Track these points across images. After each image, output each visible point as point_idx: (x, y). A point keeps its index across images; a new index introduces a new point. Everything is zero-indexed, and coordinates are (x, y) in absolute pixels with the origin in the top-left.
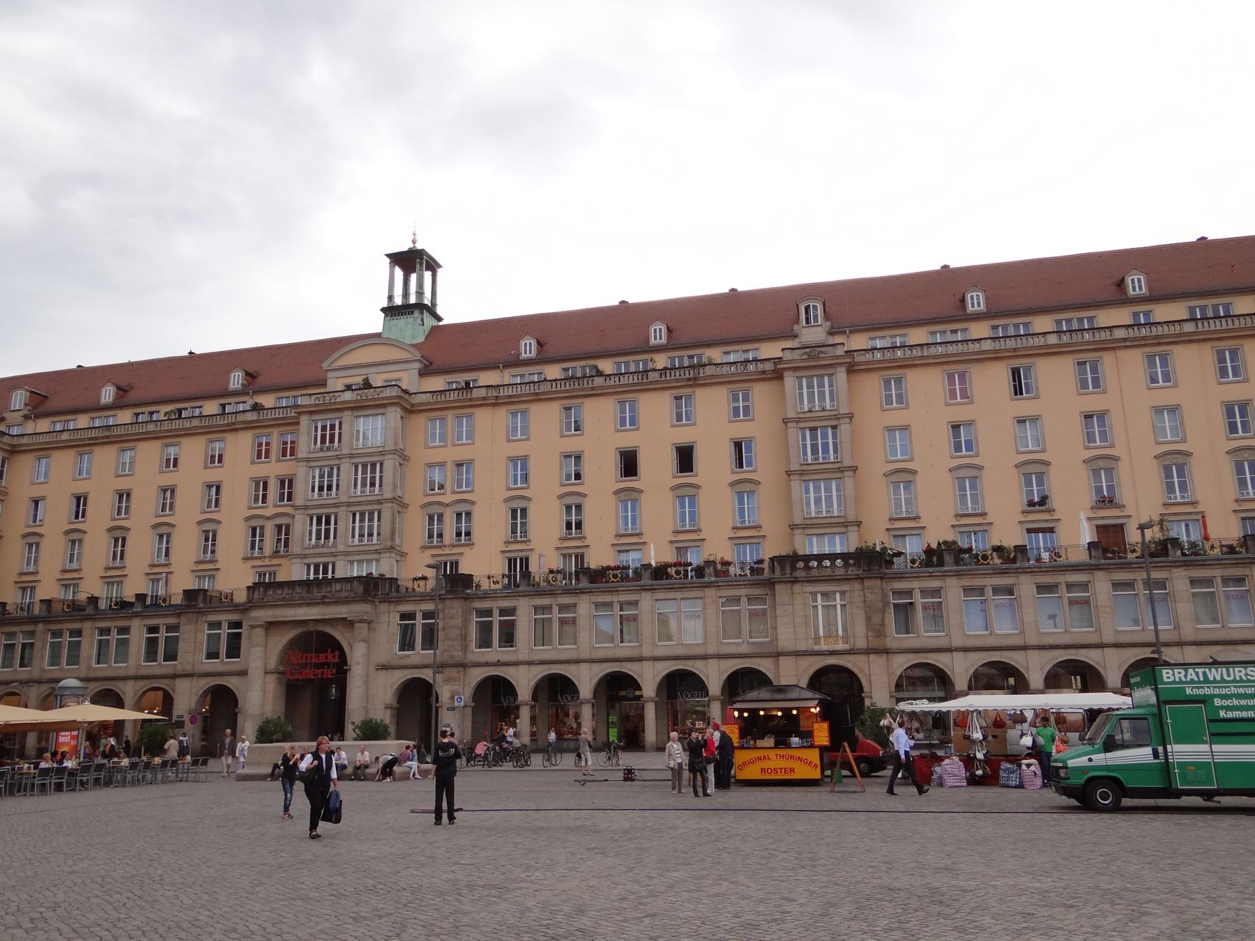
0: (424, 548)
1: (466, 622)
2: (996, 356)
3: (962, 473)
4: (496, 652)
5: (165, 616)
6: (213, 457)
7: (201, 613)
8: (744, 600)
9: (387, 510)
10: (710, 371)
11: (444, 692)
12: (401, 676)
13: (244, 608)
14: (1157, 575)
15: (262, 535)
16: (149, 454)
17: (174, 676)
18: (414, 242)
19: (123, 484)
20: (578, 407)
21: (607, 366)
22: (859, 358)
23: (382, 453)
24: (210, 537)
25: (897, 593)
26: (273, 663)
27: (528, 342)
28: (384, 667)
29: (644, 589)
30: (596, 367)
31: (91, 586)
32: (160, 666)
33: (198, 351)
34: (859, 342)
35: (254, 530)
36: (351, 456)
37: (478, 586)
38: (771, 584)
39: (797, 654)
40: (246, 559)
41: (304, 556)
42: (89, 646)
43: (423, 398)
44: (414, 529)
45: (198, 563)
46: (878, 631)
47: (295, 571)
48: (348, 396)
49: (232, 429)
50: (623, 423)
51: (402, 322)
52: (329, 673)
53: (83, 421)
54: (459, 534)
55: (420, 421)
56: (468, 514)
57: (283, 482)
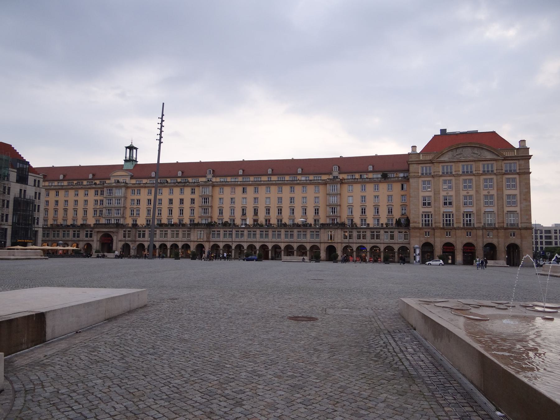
0: (130, 217)
1: (136, 233)
2: (240, 185)
3: (232, 208)
4: (141, 239)
5: (77, 229)
6: (86, 194)
7: (84, 229)
8: (186, 231)
9: (122, 209)
10: (188, 184)
11: (131, 246)
12: (123, 243)
13: (93, 228)
15: (97, 212)
16: (72, 193)
17: (79, 241)
18: (132, 143)
19: (66, 199)
20: (162, 189)
21: (169, 180)
22: (215, 183)
23: (121, 197)
24: (85, 212)
25: (213, 231)
26: (99, 239)
28: (120, 241)
29: (169, 228)
30: (166, 180)
31: (60, 221)
32: (76, 239)
33: (82, 165)
34: (218, 179)
35: (95, 211)
36: (115, 197)
37: (139, 226)
38: (190, 228)
39: (194, 241)
40: (93, 217)
41: (105, 218)
42: (61, 234)
43: (131, 185)
44: (128, 213)
45: (83, 217)
46: (208, 238)
47: (103, 221)
48: (114, 184)
49: (89, 188)
50: (170, 193)
51: (128, 163)
52: (110, 242)
53: (56, 183)
54: (137, 214)
55: (130, 191)
56: (139, 210)
57: (101, 201)
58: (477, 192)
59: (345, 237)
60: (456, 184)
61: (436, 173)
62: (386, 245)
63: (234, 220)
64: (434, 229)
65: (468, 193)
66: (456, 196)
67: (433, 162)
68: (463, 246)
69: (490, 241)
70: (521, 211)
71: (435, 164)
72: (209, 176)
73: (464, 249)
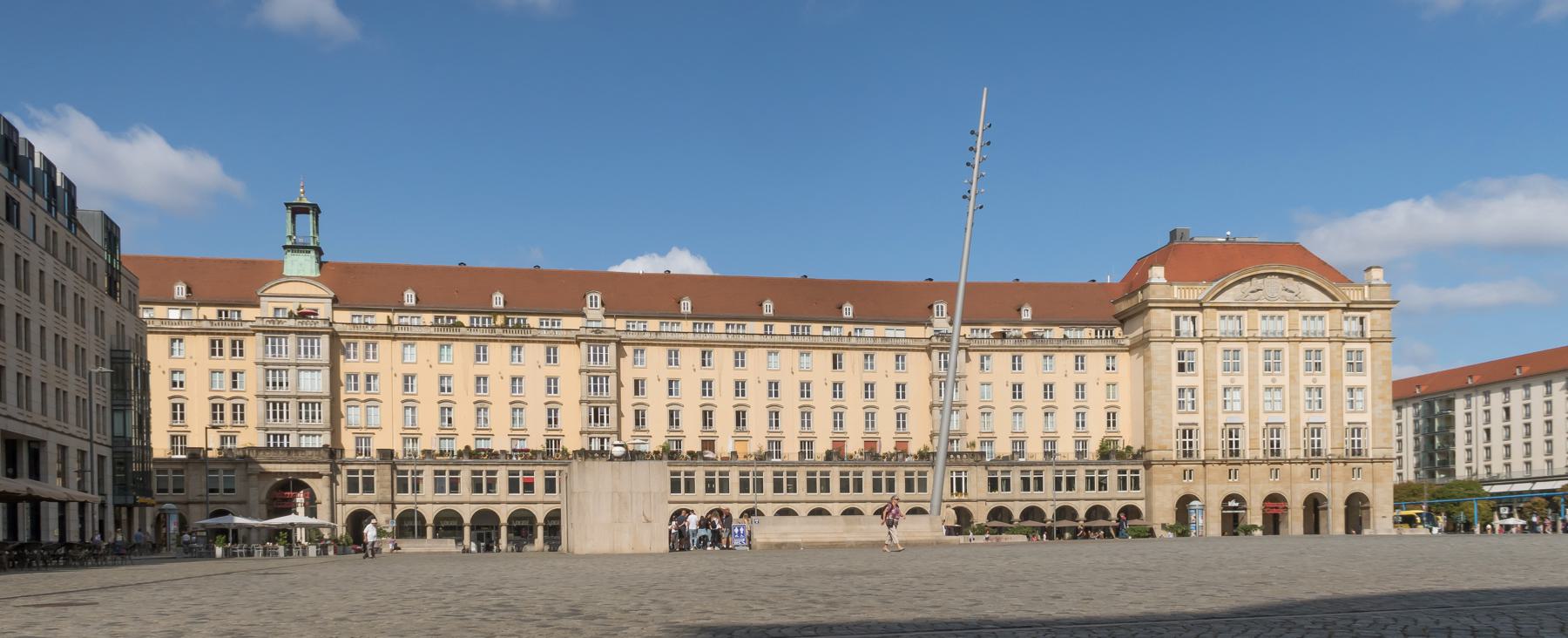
2: (695, 344)
14: (759, 469)
17: (188, 503)
26: (264, 497)
27: (409, 294)
58: (1292, 377)
59: (993, 484)
60: (1249, 359)
61: (1209, 333)
62: (1091, 504)
63: (778, 444)
64: (1204, 464)
65: (1273, 381)
66: (1251, 387)
67: (1204, 305)
68: (1264, 502)
69: (1356, 489)
70: (1373, 421)
71: (1208, 310)
72: (595, 312)
73: (1266, 508)
